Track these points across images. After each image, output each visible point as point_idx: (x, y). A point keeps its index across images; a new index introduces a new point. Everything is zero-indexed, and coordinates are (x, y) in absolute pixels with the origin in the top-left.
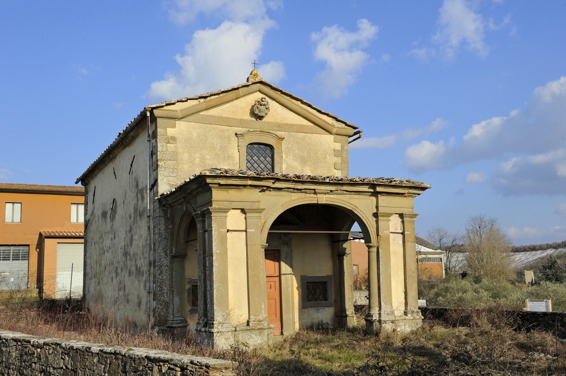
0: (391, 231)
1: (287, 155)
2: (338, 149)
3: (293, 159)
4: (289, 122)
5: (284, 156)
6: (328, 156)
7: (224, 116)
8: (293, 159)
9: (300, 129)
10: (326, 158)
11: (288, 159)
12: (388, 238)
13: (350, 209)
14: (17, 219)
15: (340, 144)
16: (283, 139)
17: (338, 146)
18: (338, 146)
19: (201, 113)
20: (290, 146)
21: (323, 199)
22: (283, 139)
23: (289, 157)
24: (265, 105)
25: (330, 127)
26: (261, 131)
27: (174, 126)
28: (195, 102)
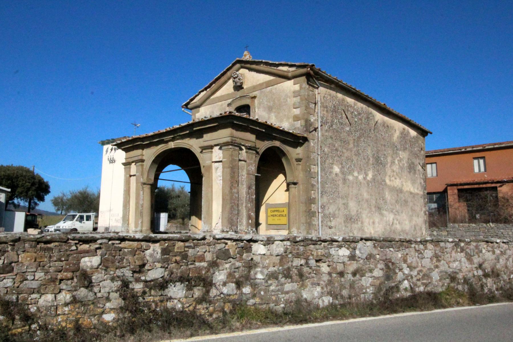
0: (214, 160)
1: (258, 108)
2: (297, 89)
3: (263, 111)
4: (261, 82)
5: (256, 110)
6: (288, 99)
7: (223, 94)
8: (263, 111)
9: (268, 84)
10: (287, 100)
11: (259, 112)
12: (210, 168)
13: (188, 148)
14: (435, 174)
15: (299, 84)
16: (255, 97)
17: (297, 87)
18: (297, 87)
19: (211, 98)
20: (261, 100)
21: (172, 145)
22: (255, 97)
23: (260, 110)
24: (236, 77)
25: (286, 74)
26: (241, 97)
27: (198, 112)
28: (205, 92)
